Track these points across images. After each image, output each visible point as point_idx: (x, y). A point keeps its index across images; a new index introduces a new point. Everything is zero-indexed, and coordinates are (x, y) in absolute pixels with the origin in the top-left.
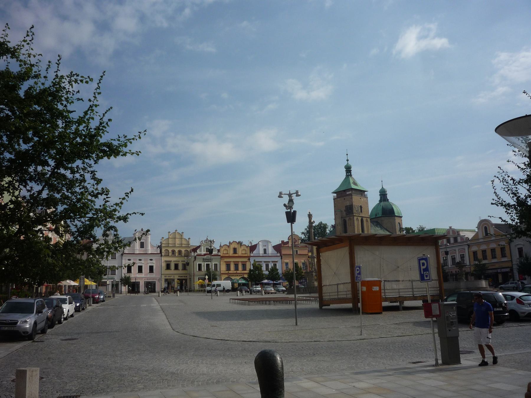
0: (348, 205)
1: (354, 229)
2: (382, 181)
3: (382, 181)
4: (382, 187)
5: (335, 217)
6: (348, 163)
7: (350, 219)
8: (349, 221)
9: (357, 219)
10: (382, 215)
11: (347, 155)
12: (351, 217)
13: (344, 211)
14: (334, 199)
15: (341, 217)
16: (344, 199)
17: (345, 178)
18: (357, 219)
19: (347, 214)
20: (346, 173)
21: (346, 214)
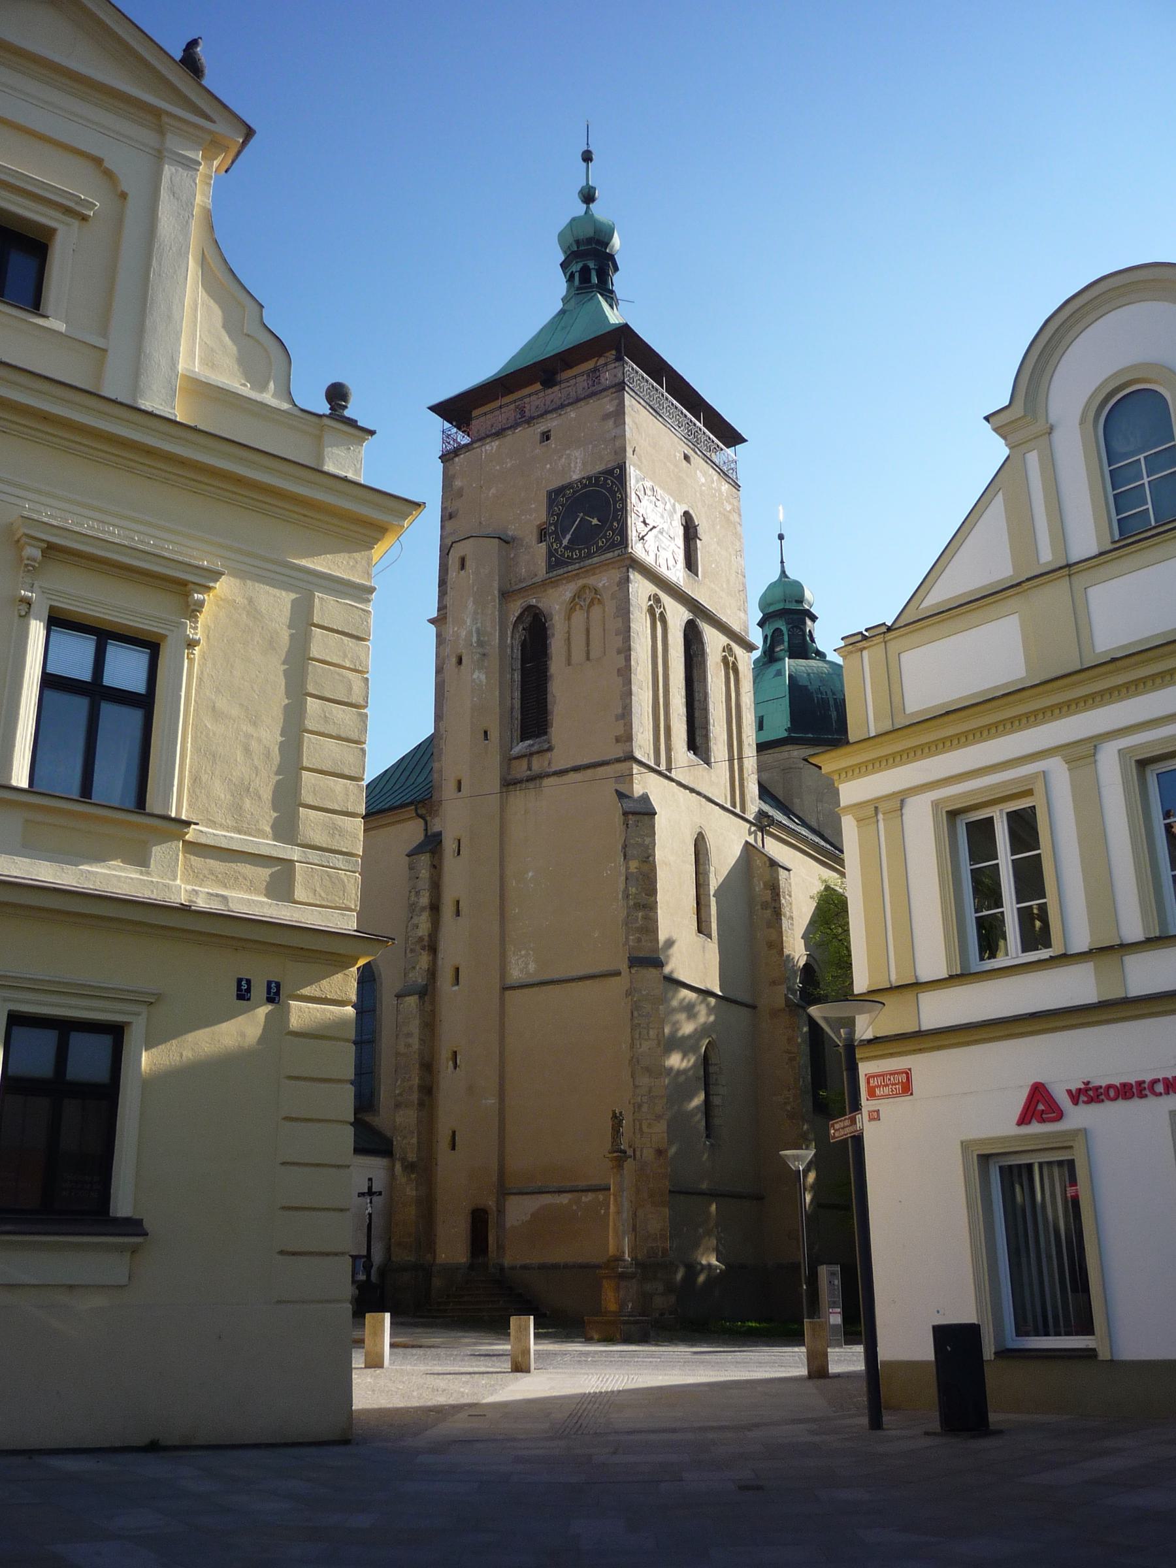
0: (575, 477)
1: (628, 682)
2: (781, 537)
3: (781, 537)
4: (783, 572)
5: (442, 608)
6: (588, 208)
7: (586, 599)
8: (579, 617)
9: (657, 617)
10: (788, 730)
11: (587, 157)
12: (604, 581)
13: (531, 537)
14: (446, 458)
15: (505, 595)
16: (546, 436)
17: (562, 312)
18: (657, 617)
19: (555, 562)
20: (570, 279)
21: (550, 553)
